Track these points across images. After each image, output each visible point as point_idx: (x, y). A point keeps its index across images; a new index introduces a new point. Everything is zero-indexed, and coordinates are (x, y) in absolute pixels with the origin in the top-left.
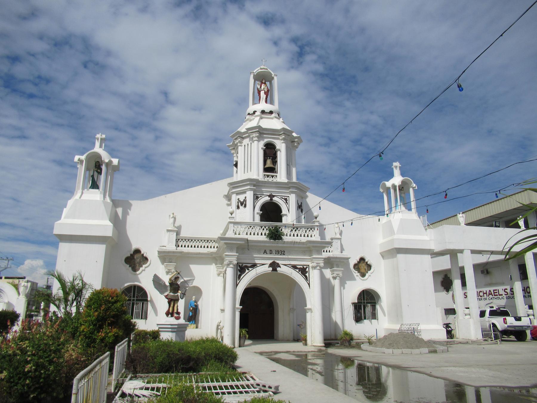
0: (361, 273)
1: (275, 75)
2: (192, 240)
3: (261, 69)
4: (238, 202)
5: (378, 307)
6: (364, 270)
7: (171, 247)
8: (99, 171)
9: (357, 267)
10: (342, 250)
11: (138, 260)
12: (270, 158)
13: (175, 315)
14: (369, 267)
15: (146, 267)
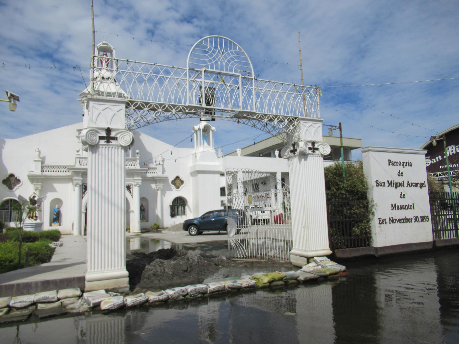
1: (113, 49)
2: (54, 167)
3: (104, 44)
5: (187, 208)
7: (38, 172)
9: (174, 182)
10: (164, 171)
11: (13, 182)
13: (34, 218)
14: (182, 182)
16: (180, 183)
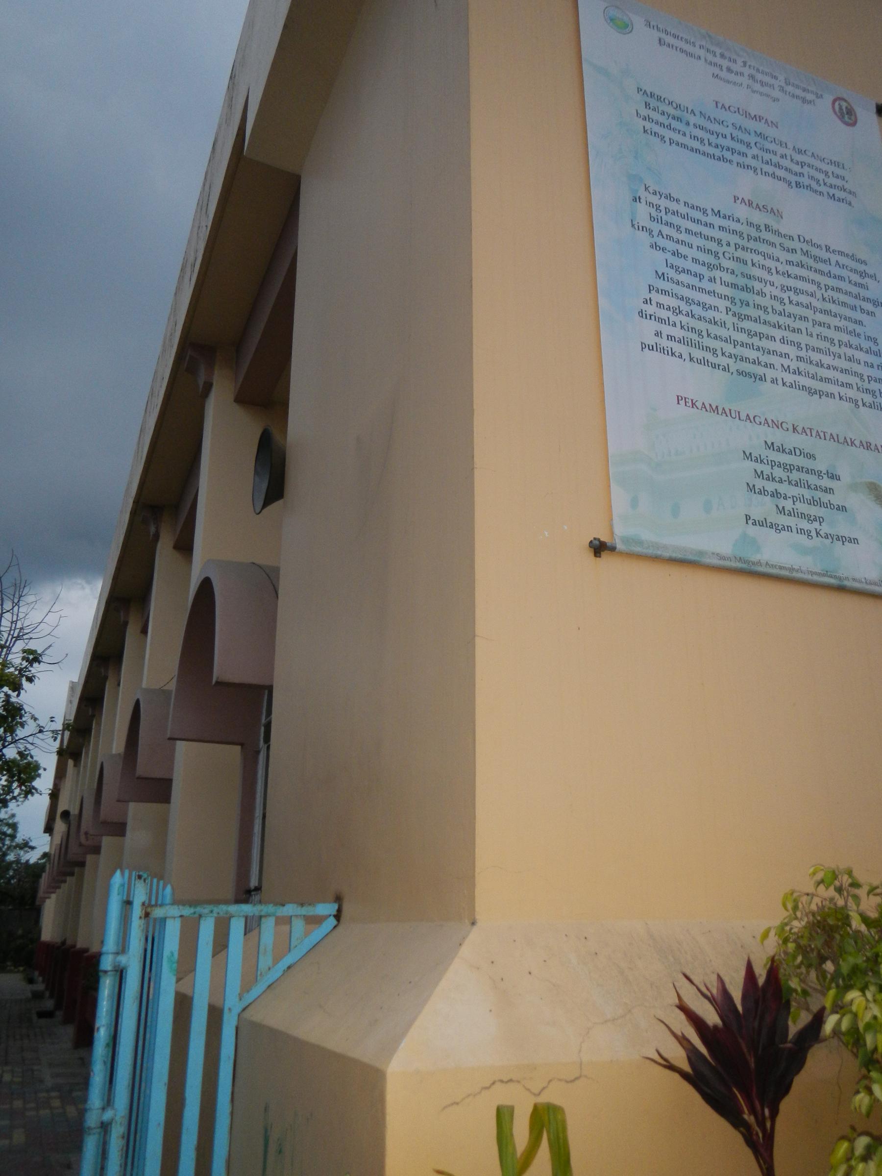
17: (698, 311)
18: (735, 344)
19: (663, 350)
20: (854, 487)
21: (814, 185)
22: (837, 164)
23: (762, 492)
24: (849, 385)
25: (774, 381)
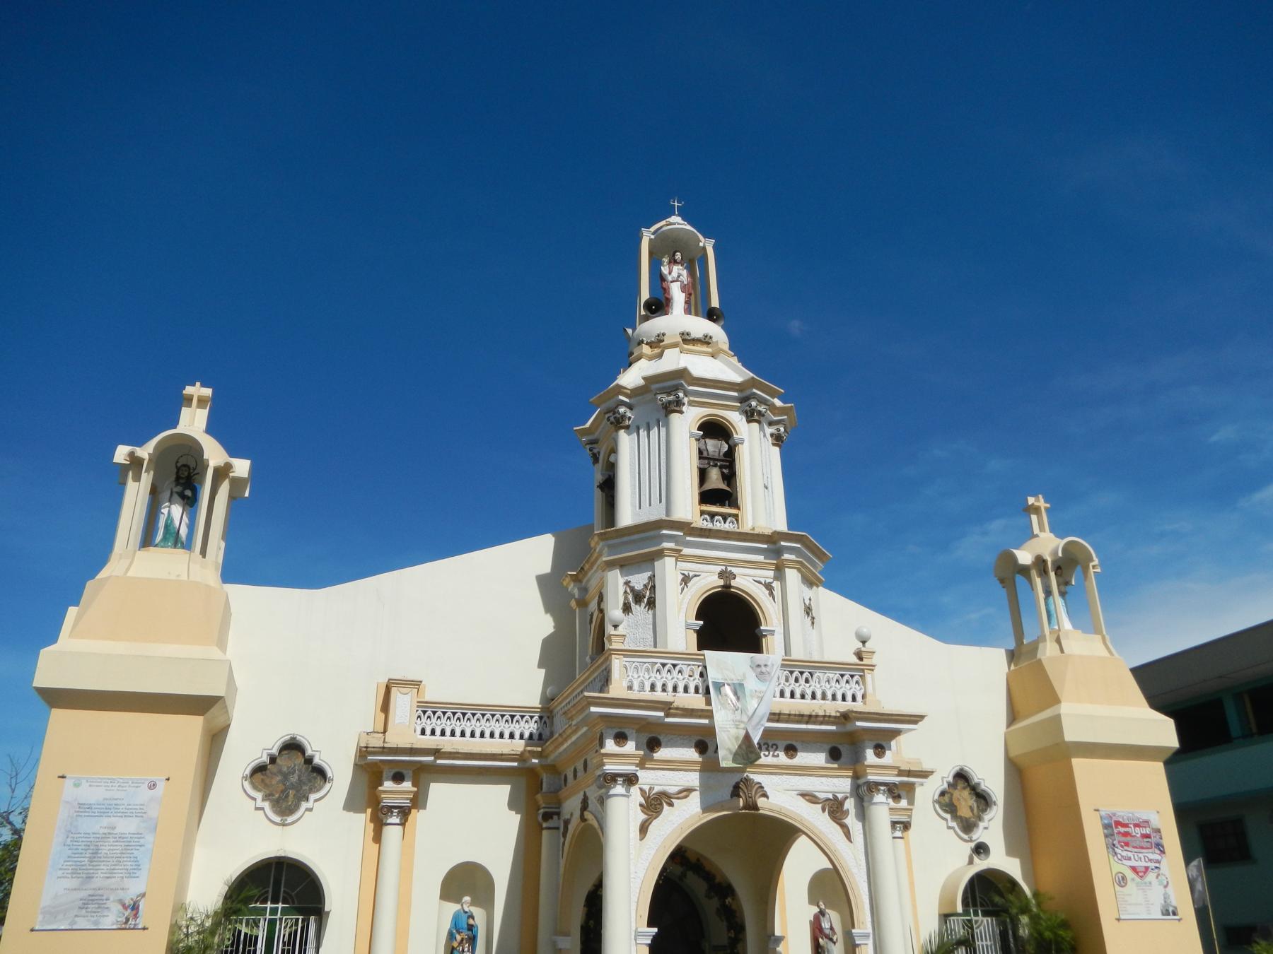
0: (962, 821)
3: (674, 224)
4: (626, 592)
6: (969, 811)
8: (188, 493)
9: (946, 798)
12: (713, 466)
15: (316, 801)
16: (972, 802)
17: (78, 863)
18: (87, 869)
19: (63, 877)
20: (114, 901)
21: (131, 815)
22: (142, 805)
23: (83, 908)
24: (122, 873)
25: (97, 877)
